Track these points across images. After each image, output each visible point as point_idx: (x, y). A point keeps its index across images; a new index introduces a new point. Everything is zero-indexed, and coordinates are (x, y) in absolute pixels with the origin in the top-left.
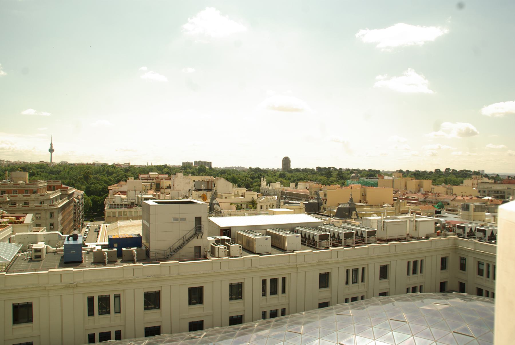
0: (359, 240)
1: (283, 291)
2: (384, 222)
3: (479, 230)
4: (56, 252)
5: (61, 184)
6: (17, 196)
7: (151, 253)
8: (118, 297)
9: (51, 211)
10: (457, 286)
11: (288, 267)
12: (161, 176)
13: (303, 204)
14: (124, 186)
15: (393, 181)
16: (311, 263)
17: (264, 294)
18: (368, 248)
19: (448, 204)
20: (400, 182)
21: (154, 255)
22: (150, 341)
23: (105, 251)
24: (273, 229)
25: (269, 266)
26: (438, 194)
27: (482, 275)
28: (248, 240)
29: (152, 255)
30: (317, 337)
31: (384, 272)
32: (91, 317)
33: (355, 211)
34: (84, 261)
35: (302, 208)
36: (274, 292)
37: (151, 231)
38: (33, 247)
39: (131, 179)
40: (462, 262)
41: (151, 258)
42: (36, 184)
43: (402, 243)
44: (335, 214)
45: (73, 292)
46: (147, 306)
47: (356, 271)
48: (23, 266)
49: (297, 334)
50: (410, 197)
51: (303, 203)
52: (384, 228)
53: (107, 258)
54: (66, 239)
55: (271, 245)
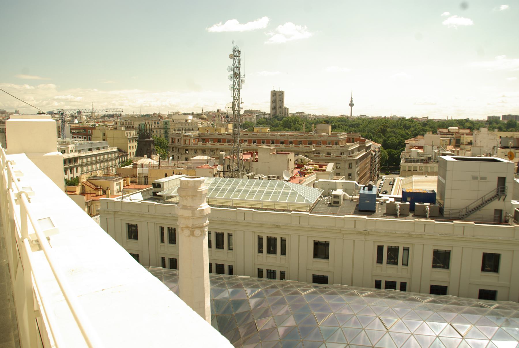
4: (352, 200)
5: (360, 137)
7: (445, 210)
8: (406, 250)
9: (349, 162)
12: (461, 131)
14: (421, 141)
21: (448, 213)
22: (435, 299)
23: (398, 204)
29: (446, 213)
32: (379, 265)
34: (377, 212)
37: (446, 188)
38: (333, 193)
39: (429, 133)
41: (444, 216)
42: (337, 136)
45: (365, 239)
46: (435, 264)
48: (324, 209)
53: (399, 210)
54: (362, 188)
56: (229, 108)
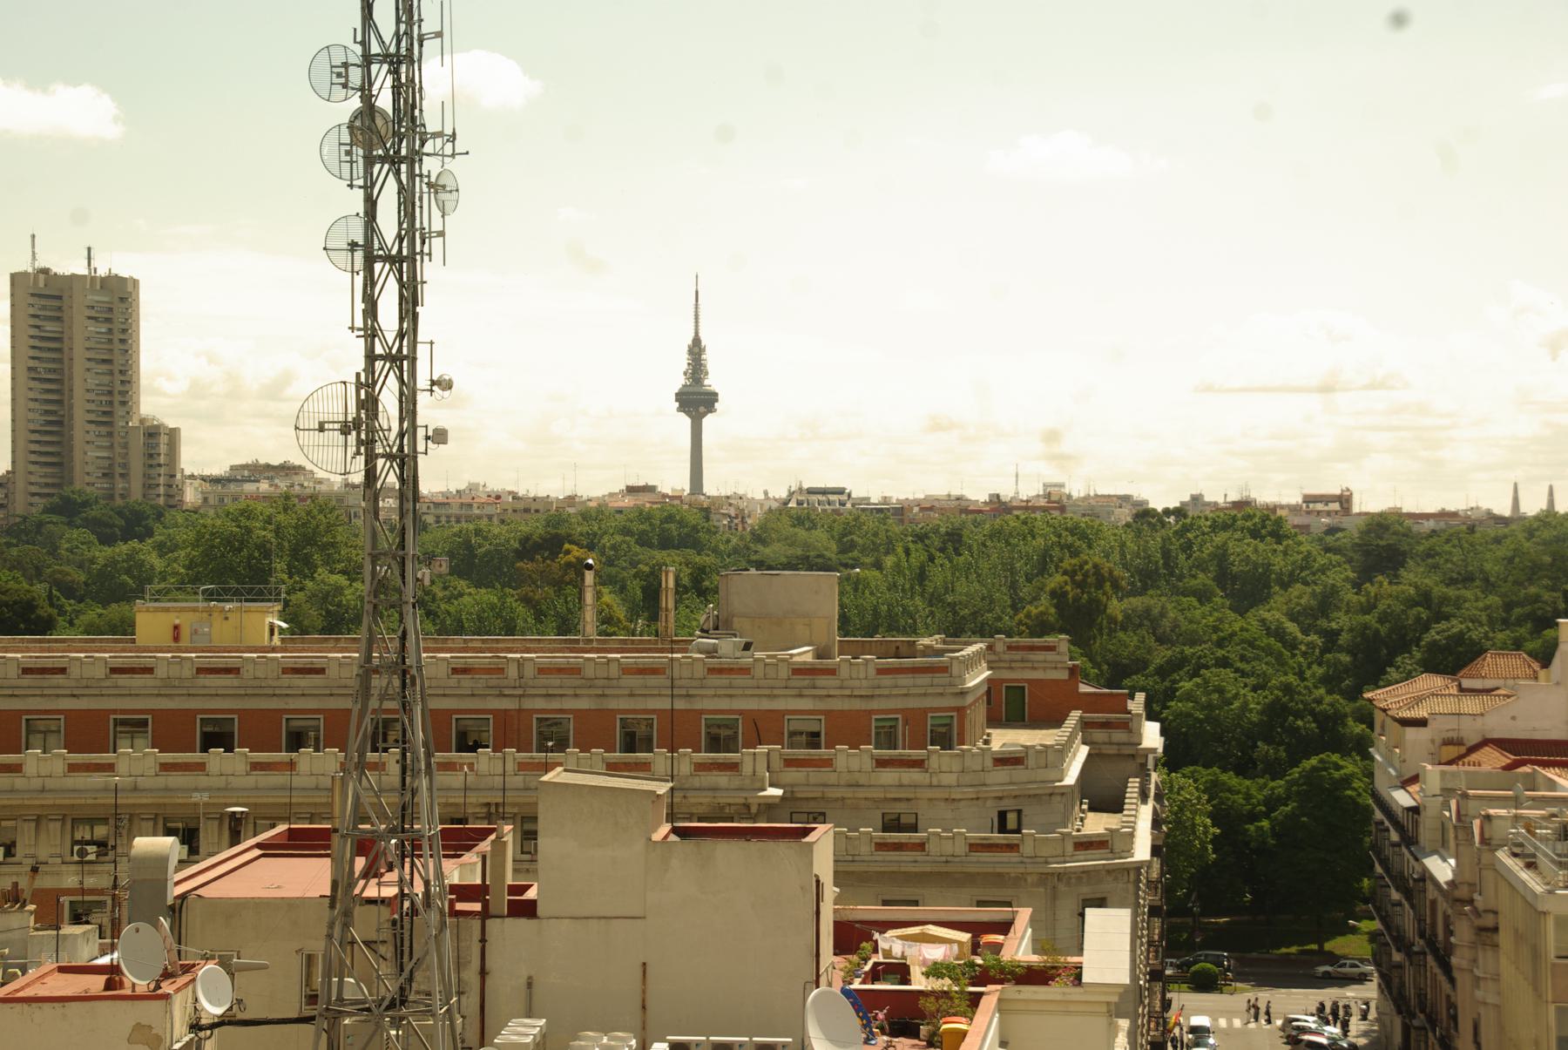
6: (828, 763)
42: (944, 669)
56: (321, 429)
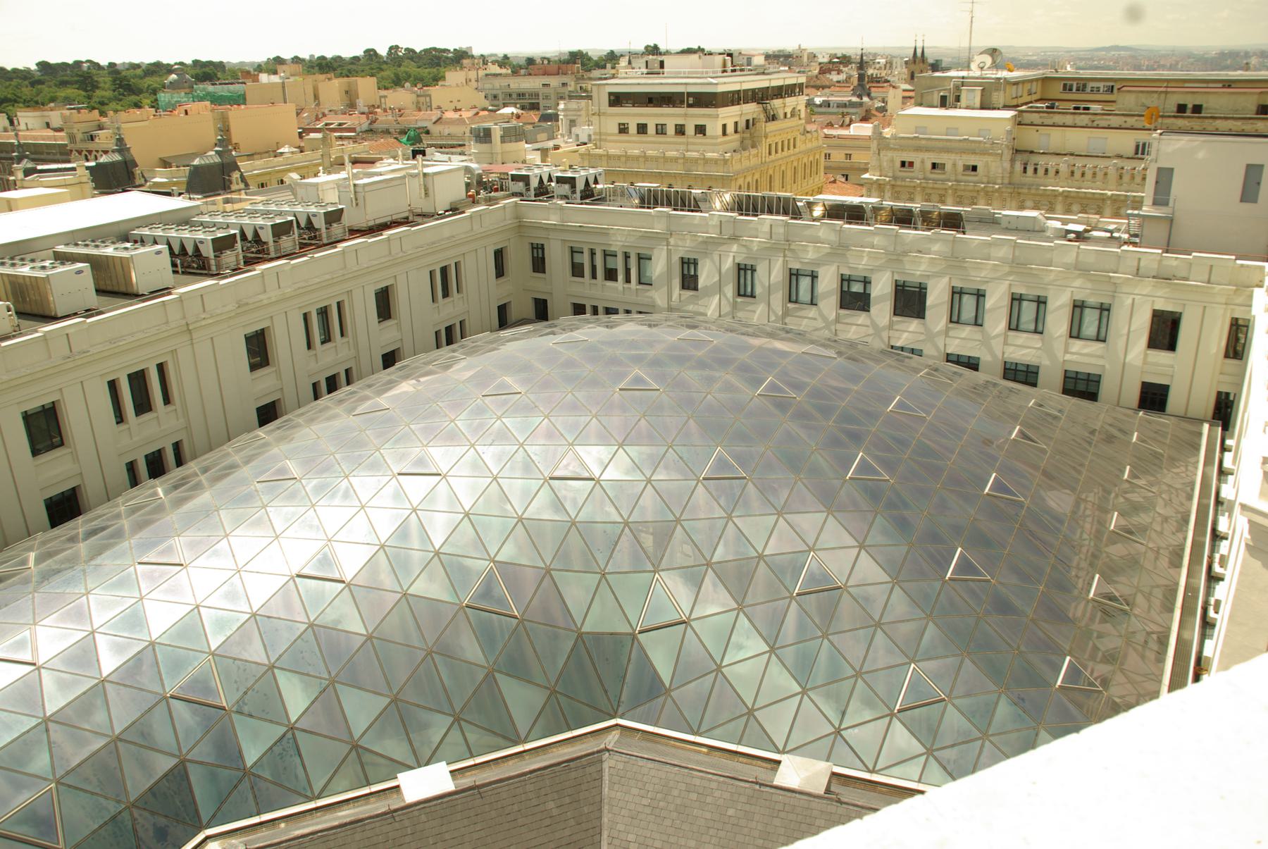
0: (305, 239)
1: (167, 400)
2: (355, 185)
3: (560, 180)
10: (530, 311)
11: (166, 334)
13: (84, 168)
15: (283, 87)
16: (221, 314)
17: (120, 418)
18: (343, 252)
19: (428, 132)
20: (302, 85)
24: (76, 245)
25: (120, 341)
26: (400, 111)
27: (582, 276)
28: (19, 284)
30: (338, 475)
31: (385, 304)
33: (237, 171)
35: (85, 179)
36: (143, 405)
40: (535, 255)
43: (413, 229)
44: (184, 186)
47: (324, 312)
49: (289, 481)
50: (332, 124)
51: (81, 167)
52: (356, 199)
55: (97, 291)
